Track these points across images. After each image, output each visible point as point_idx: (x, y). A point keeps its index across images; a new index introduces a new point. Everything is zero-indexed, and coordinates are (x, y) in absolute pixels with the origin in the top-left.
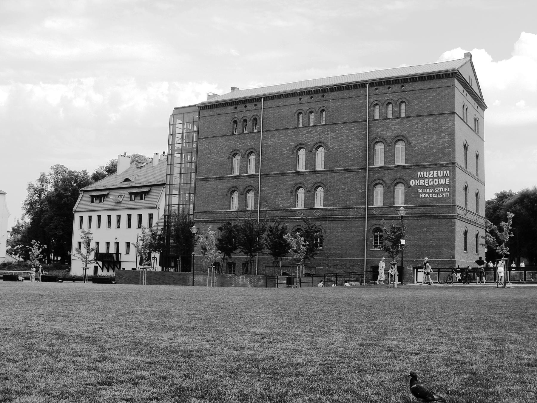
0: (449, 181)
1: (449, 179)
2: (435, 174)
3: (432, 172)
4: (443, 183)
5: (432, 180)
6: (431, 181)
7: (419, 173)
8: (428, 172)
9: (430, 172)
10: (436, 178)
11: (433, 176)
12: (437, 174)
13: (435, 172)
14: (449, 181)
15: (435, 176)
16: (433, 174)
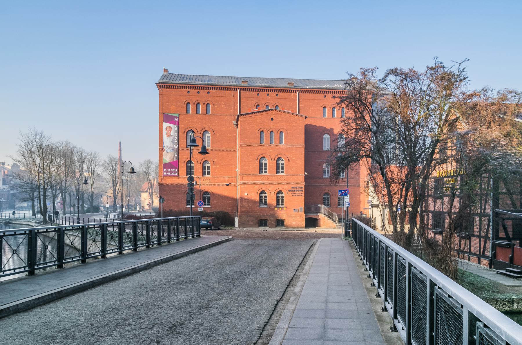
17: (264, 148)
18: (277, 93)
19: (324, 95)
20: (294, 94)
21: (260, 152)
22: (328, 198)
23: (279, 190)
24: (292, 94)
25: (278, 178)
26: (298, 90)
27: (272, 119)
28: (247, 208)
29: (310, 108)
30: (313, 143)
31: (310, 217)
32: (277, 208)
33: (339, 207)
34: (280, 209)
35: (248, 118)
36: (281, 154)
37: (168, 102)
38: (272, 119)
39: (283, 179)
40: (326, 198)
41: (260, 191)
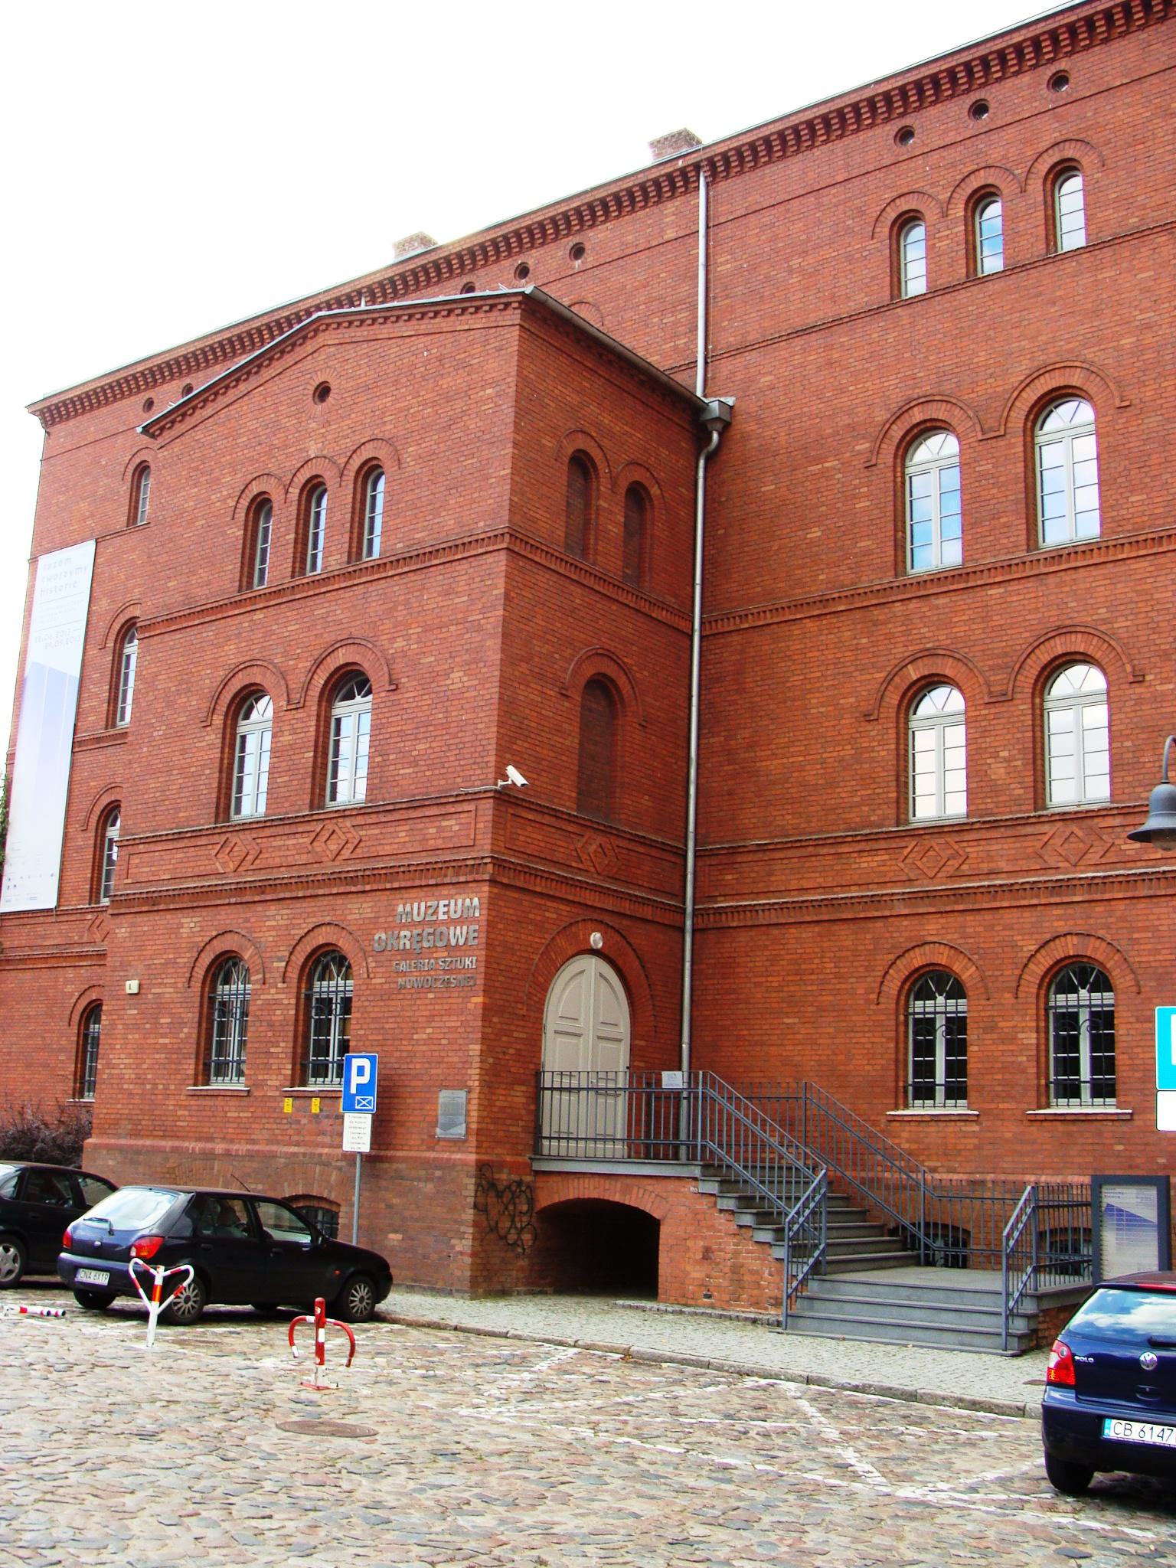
0: (476, 935)
1: (477, 927)
2: (442, 909)
3: (435, 903)
4: (461, 942)
5: (431, 930)
6: (429, 934)
7: (400, 909)
8: (423, 905)
9: (429, 904)
10: (443, 922)
11: (434, 918)
12: (446, 909)
13: (442, 903)
14: (476, 935)
15: (442, 917)
16: (435, 912)
17: (259, 615)
18: (572, 241)
19: (893, 127)
20: (677, 202)
21: (232, 653)
22: (957, 1025)
23: (321, 938)
24: (670, 207)
25: (318, 846)
26: (697, 167)
27: (323, 392)
28: (131, 1094)
29: (795, 262)
30: (815, 533)
31: (594, 1195)
32: (296, 1097)
33: (1063, 1107)
34: (315, 1105)
35: (198, 434)
36: (349, 641)
37: (67, 491)
38: (323, 392)
39: (350, 846)
40: (940, 1021)
41: (206, 959)
